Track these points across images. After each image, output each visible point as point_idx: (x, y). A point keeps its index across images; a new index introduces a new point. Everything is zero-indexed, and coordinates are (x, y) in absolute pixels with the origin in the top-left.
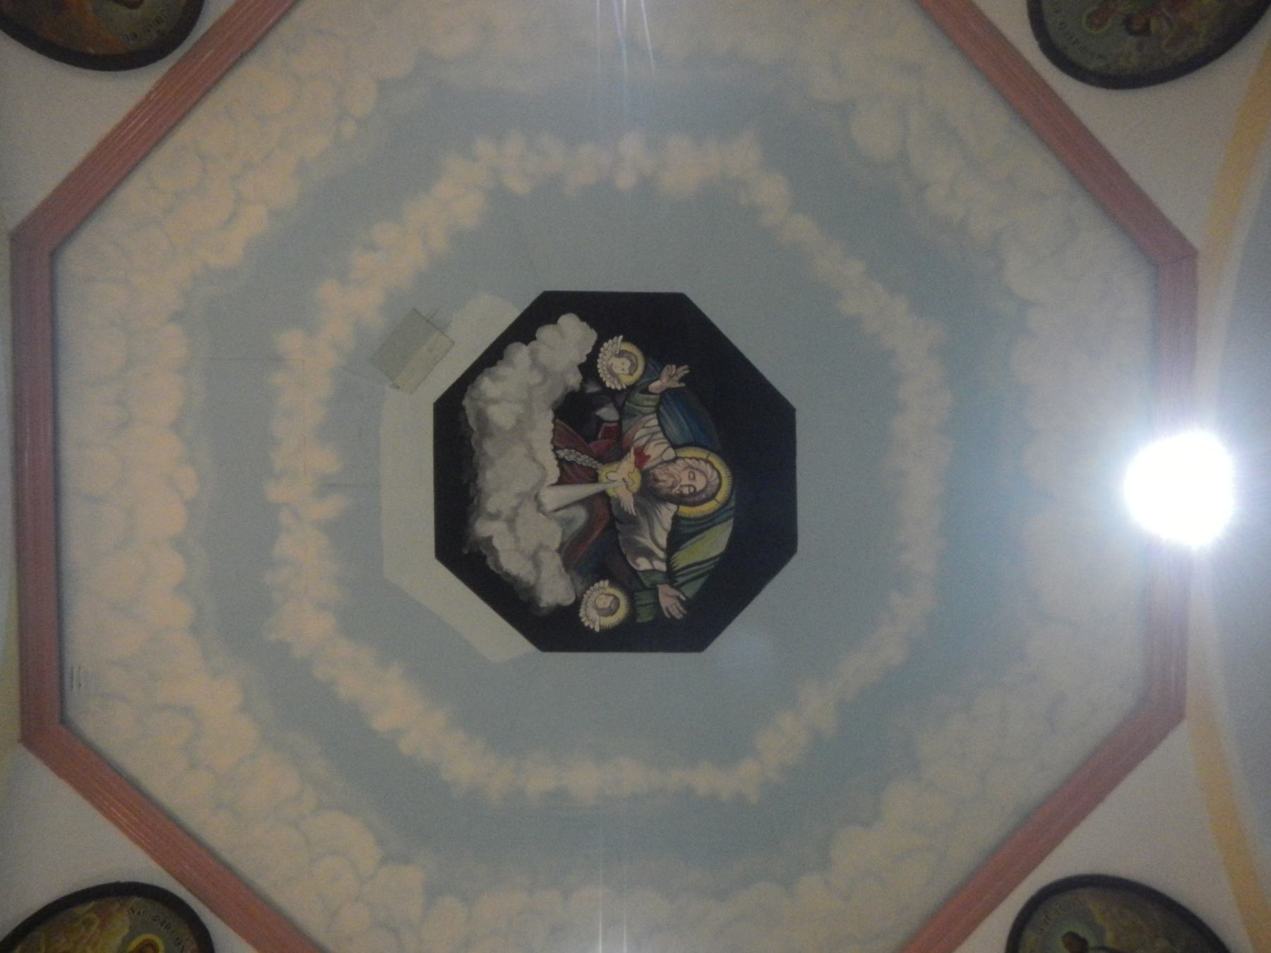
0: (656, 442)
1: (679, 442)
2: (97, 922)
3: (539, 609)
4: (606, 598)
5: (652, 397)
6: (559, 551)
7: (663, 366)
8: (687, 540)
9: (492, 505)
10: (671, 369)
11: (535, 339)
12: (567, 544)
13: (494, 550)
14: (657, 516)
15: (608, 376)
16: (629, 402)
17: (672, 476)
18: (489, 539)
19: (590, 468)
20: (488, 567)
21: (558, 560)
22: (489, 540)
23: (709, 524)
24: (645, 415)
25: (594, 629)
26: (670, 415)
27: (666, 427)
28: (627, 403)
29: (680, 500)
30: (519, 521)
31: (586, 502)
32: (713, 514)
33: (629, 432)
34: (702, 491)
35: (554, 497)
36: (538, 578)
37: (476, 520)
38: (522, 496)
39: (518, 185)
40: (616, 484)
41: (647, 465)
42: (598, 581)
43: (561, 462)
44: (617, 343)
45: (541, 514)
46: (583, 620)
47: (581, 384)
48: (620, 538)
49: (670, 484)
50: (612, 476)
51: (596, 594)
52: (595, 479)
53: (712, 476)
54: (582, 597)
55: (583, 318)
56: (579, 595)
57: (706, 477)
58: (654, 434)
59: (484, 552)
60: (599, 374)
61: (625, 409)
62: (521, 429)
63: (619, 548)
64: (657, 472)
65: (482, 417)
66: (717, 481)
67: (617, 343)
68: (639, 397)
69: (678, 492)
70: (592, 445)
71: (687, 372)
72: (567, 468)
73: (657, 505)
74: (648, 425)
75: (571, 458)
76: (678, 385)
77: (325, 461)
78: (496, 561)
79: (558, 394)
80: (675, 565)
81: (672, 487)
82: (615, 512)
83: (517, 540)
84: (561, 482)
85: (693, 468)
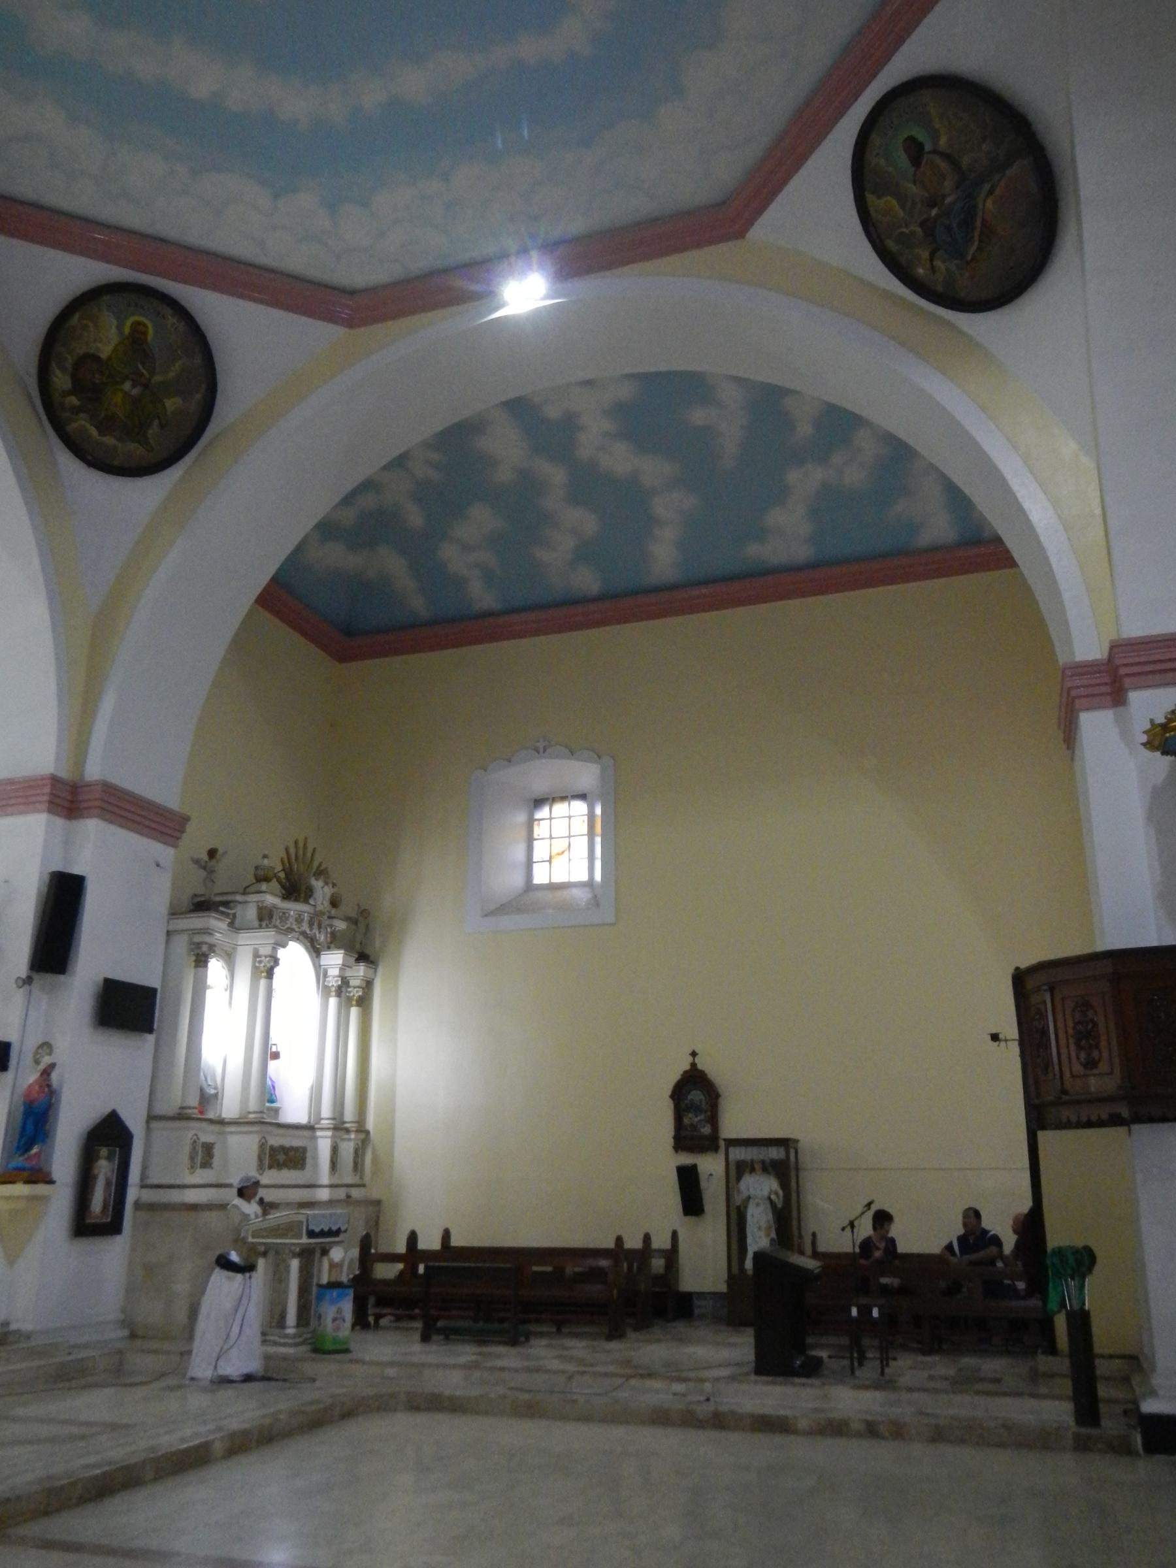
2: (91, 325)
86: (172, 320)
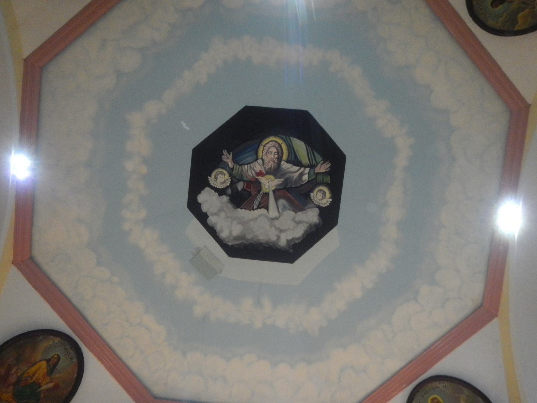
0: (254, 166)
1: (255, 157)
3: (319, 223)
4: (318, 195)
5: (235, 166)
6: (296, 212)
7: (222, 161)
8: (297, 157)
9: (273, 238)
10: (224, 158)
11: (206, 213)
12: (293, 209)
13: (293, 239)
14: (285, 170)
15: (225, 184)
16: (236, 176)
17: (269, 162)
18: (288, 241)
19: (263, 195)
20: (299, 243)
21: (300, 213)
22: (288, 241)
23: (292, 149)
24: (242, 170)
25: (330, 201)
26: (244, 160)
27: (248, 162)
28: (236, 178)
29: (280, 159)
30: (281, 228)
31: (277, 199)
32: (287, 145)
33: (249, 178)
34: (277, 149)
35: (273, 212)
36: (306, 222)
37: (279, 245)
38: (272, 225)
39: (143, 214)
40: (270, 186)
41: (264, 172)
42: (310, 197)
43: (259, 207)
44: (211, 179)
45: (280, 218)
46: (326, 206)
47: (227, 196)
48: (293, 186)
49: (272, 163)
50: (267, 187)
51: (316, 199)
52: (267, 194)
53: (271, 144)
54: (317, 205)
55: (200, 192)
56: (315, 206)
57: (271, 147)
58: (250, 166)
59: (293, 243)
60: (223, 188)
61: (239, 178)
62: (244, 223)
63: (297, 187)
64: (267, 167)
65: (236, 238)
66: (274, 142)
67: (211, 179)
68: (234, 172)
69: (276, 160)
70: (253, 194)
71: (226, 151)
72: (261, 206)
73: (281, 169)
74: (247, 170)
75: (257, 203)
76: (231, 156)
77: (248, 303)
78: (297, 239)
79: (230, 206)
80: (307, 164)
81: (274, 162)
82: (282, 187)
83: (289, 229)
84: (267, 208)
85: (267, 152)
86: (440, 385)
